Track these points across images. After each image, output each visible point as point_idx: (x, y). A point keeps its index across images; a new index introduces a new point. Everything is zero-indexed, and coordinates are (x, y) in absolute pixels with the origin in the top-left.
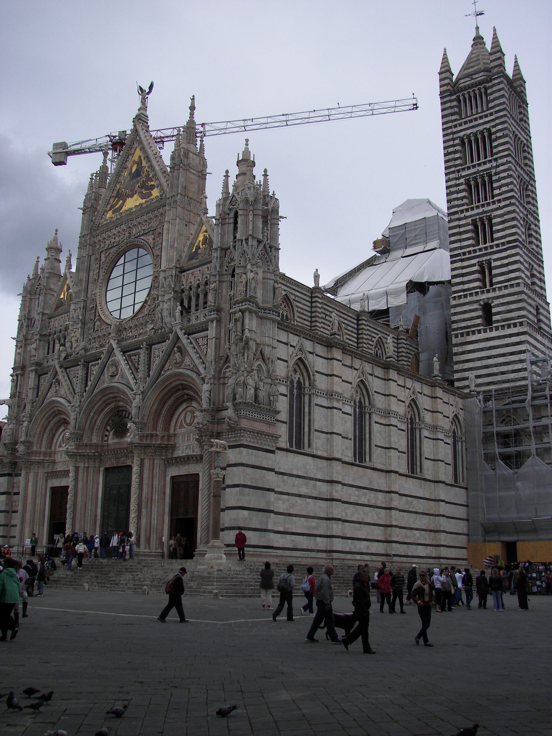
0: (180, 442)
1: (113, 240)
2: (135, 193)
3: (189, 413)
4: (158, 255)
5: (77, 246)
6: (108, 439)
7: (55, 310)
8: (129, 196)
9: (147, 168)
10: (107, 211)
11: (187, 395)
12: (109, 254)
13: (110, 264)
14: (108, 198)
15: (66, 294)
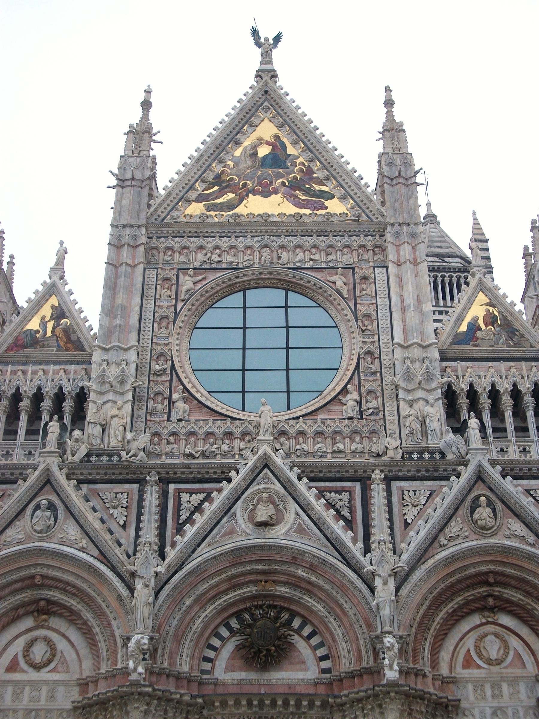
0: (472, 698)
1: (215, 258)
2: (276, 192)
3: (491, 637)
4: (367, 316)
5: (107, 239)
6: (213, 667)
7: (7, 350)
8: (254, 192)
9: (301, 159)
10: (189, 201)
11: (496, 598)
12: (204, 279)
13: (207, 298)
14: (193, 180)
15: (50, 325)
